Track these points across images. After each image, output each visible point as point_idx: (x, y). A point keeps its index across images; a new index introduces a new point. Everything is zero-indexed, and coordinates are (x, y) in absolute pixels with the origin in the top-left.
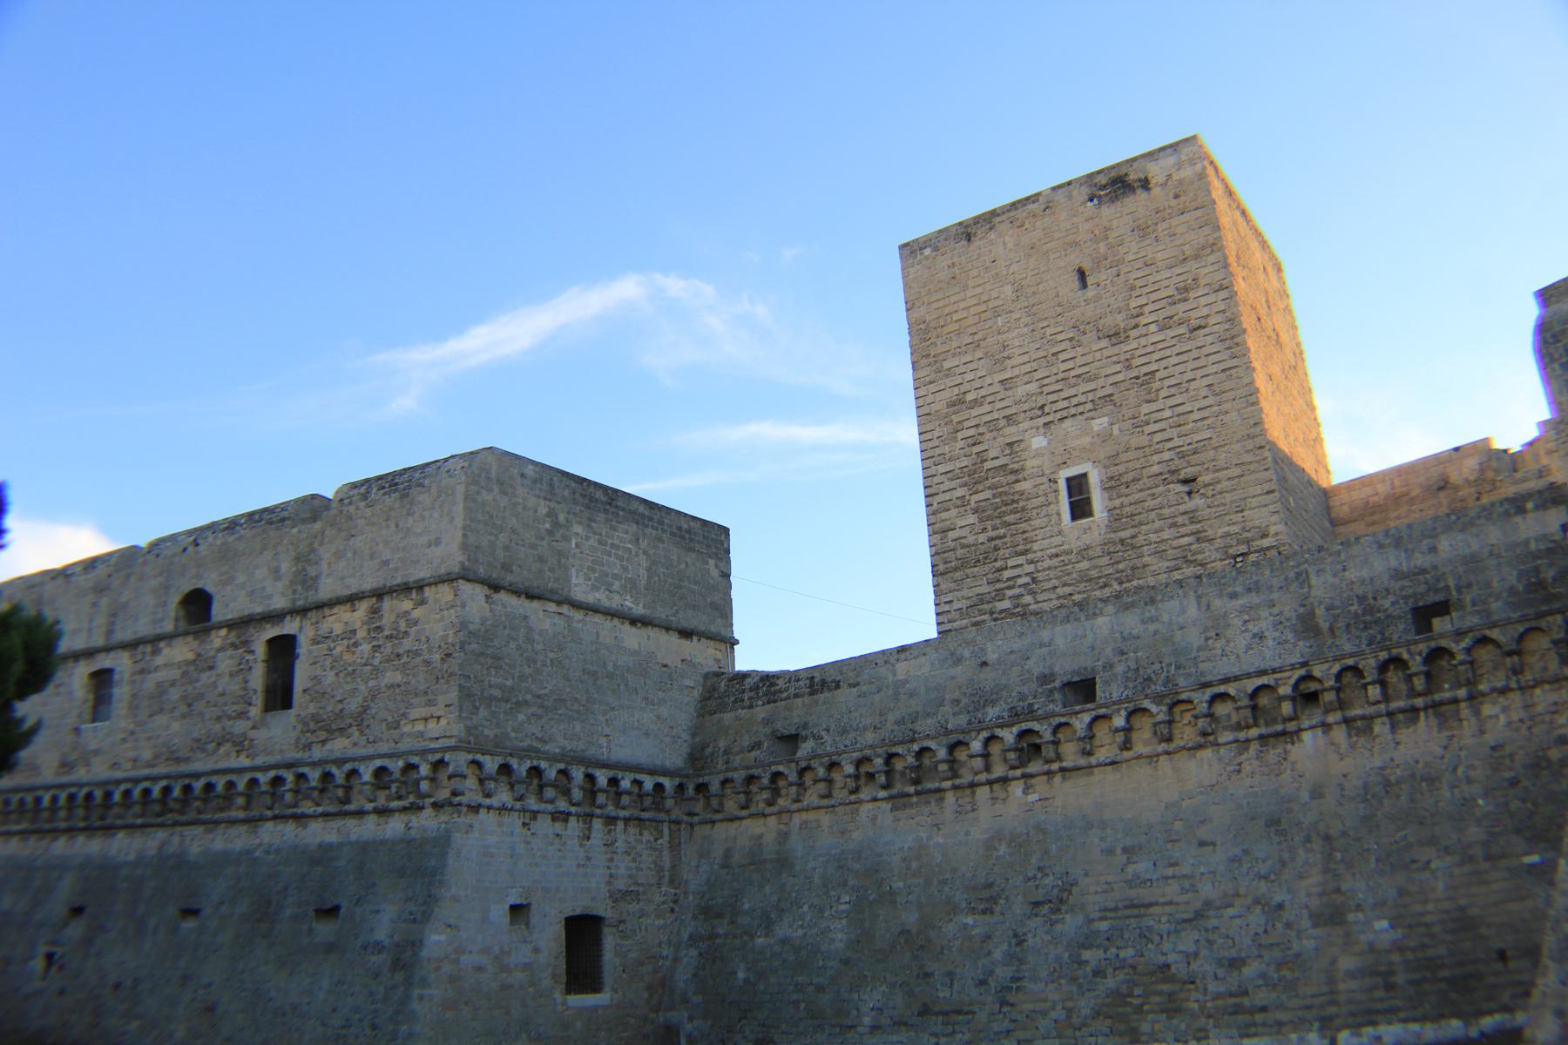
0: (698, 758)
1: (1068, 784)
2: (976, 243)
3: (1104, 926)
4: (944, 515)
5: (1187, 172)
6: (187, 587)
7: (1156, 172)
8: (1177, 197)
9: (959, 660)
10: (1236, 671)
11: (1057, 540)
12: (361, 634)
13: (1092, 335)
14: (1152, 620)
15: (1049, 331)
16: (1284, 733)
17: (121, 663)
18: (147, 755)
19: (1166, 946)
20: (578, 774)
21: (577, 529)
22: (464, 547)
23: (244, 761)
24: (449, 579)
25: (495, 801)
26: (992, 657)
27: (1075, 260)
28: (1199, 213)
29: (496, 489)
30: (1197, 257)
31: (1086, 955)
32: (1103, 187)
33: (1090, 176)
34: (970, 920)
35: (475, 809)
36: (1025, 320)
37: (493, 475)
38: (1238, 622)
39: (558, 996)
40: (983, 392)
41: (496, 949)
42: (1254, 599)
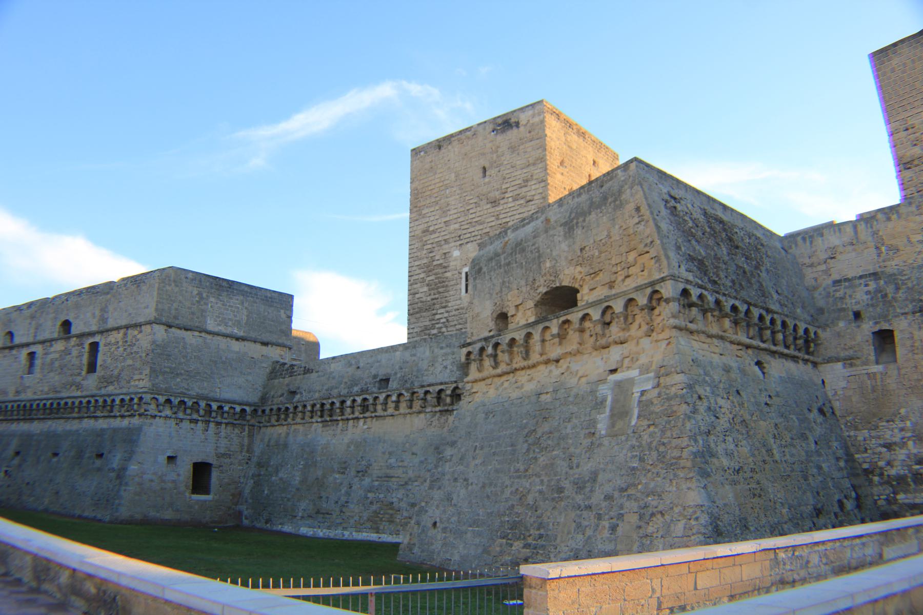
0: (264, 399)
2: (443, 150)
3: (376, 483)
4: (415, 286)
5: (536, 119)
6: (63, 319)
7: (523, 118)
8: (530, 132)
9: (351, 365)
10: (434, 382)
11: (458, 302)
12: (120, 343)
13: (485, 201)
14: (414, 355)
15: (467, 198)
16: (447, 411)
17: (38, 349)
18: (46, 389)
19: (394, 495)
20: (203, 404)
21: (212, 299)
22: (156, 310)
23: (79, 394)
24: (150, 323)
25: (163, 414)
26: (361, 365)
27: (483, 162)
28: (538, 141)
30: (534, 164)
31: (370, 495)
32: (499, 125)
33: (495, 119)
34: (337, 476)
35: (154, 417)
36: (458, 192)
37: (172, 279)
38: (440, 360)
39: (187, 494)
40: (436, 227)
41: (160, 473)
42: (448, 350)
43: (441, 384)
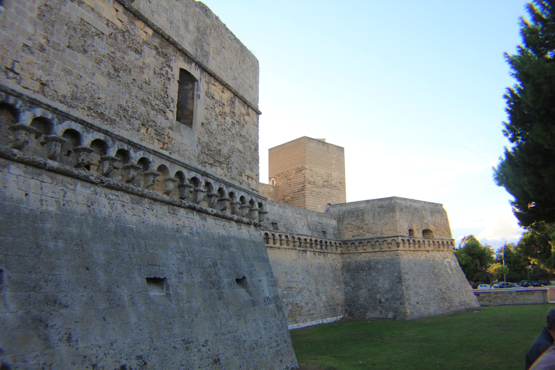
1: (271, 251)
3: (285, 292)
43: (306, 236)
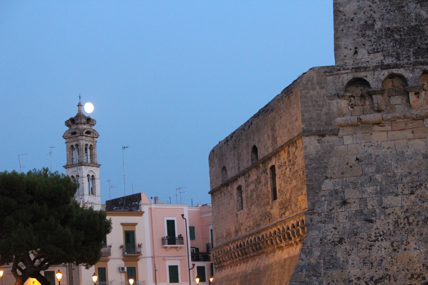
12: (287, 164)
22: (303, 121)
29: (317, 87)
37: (315, 81)
